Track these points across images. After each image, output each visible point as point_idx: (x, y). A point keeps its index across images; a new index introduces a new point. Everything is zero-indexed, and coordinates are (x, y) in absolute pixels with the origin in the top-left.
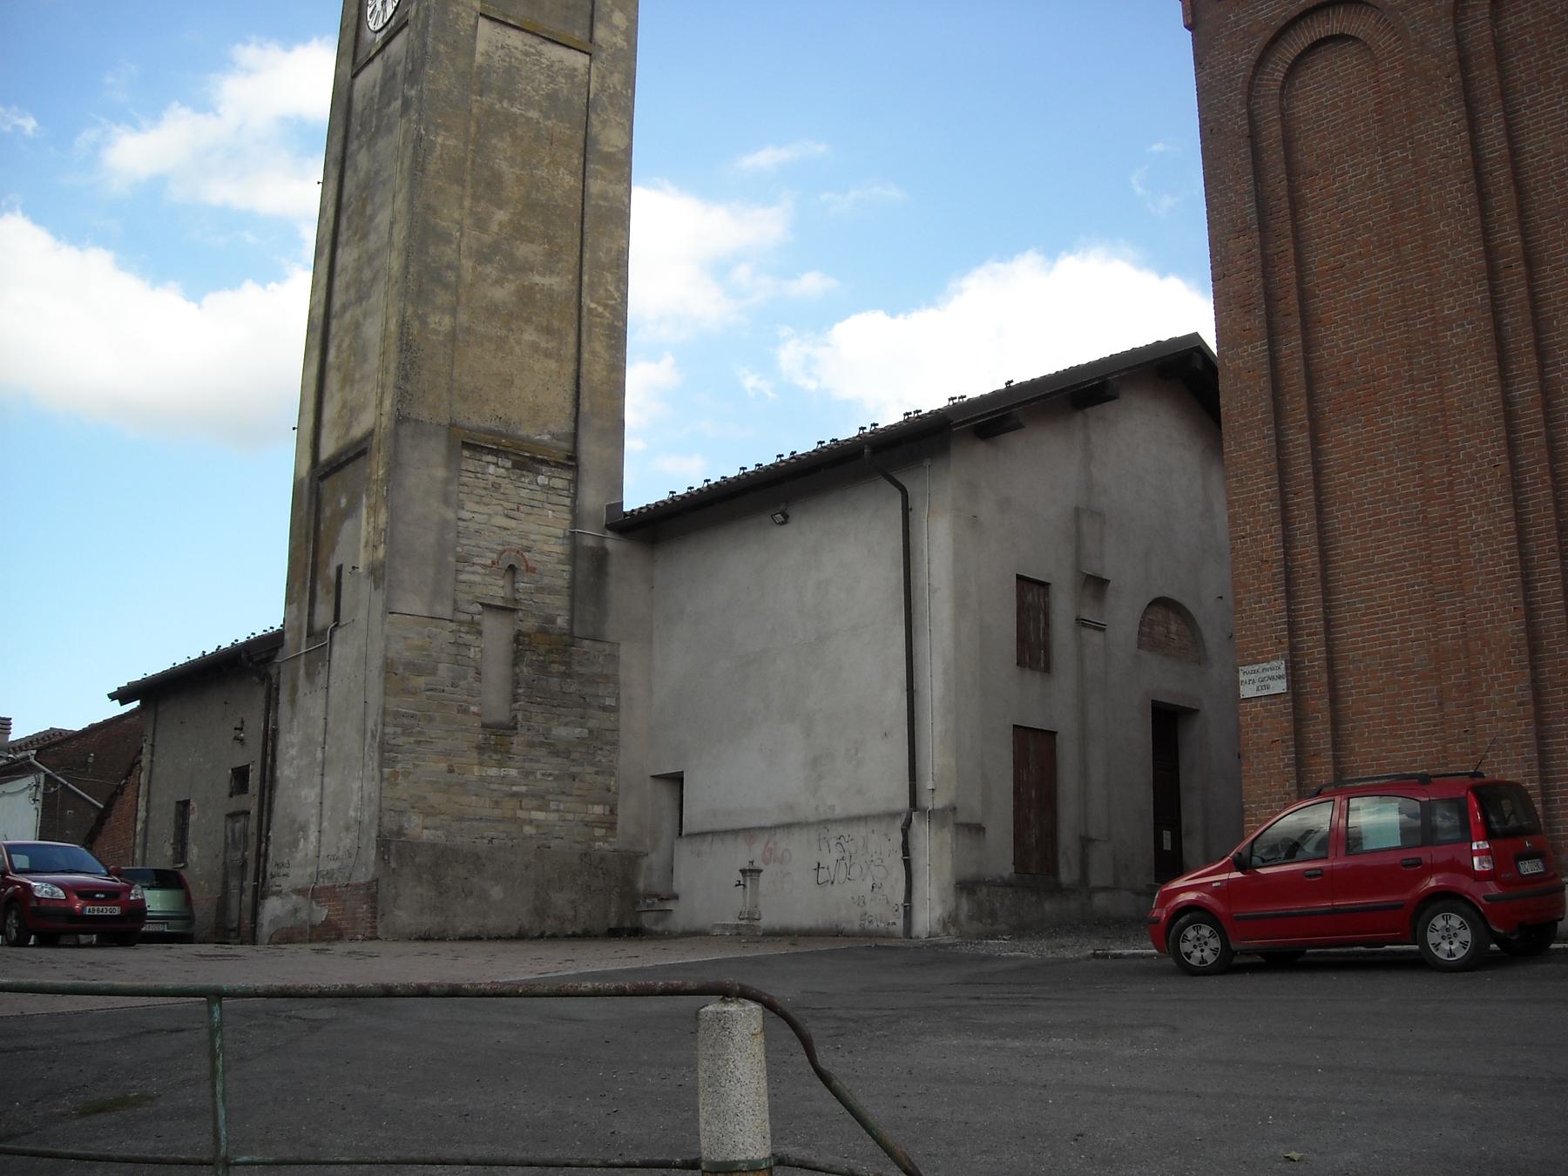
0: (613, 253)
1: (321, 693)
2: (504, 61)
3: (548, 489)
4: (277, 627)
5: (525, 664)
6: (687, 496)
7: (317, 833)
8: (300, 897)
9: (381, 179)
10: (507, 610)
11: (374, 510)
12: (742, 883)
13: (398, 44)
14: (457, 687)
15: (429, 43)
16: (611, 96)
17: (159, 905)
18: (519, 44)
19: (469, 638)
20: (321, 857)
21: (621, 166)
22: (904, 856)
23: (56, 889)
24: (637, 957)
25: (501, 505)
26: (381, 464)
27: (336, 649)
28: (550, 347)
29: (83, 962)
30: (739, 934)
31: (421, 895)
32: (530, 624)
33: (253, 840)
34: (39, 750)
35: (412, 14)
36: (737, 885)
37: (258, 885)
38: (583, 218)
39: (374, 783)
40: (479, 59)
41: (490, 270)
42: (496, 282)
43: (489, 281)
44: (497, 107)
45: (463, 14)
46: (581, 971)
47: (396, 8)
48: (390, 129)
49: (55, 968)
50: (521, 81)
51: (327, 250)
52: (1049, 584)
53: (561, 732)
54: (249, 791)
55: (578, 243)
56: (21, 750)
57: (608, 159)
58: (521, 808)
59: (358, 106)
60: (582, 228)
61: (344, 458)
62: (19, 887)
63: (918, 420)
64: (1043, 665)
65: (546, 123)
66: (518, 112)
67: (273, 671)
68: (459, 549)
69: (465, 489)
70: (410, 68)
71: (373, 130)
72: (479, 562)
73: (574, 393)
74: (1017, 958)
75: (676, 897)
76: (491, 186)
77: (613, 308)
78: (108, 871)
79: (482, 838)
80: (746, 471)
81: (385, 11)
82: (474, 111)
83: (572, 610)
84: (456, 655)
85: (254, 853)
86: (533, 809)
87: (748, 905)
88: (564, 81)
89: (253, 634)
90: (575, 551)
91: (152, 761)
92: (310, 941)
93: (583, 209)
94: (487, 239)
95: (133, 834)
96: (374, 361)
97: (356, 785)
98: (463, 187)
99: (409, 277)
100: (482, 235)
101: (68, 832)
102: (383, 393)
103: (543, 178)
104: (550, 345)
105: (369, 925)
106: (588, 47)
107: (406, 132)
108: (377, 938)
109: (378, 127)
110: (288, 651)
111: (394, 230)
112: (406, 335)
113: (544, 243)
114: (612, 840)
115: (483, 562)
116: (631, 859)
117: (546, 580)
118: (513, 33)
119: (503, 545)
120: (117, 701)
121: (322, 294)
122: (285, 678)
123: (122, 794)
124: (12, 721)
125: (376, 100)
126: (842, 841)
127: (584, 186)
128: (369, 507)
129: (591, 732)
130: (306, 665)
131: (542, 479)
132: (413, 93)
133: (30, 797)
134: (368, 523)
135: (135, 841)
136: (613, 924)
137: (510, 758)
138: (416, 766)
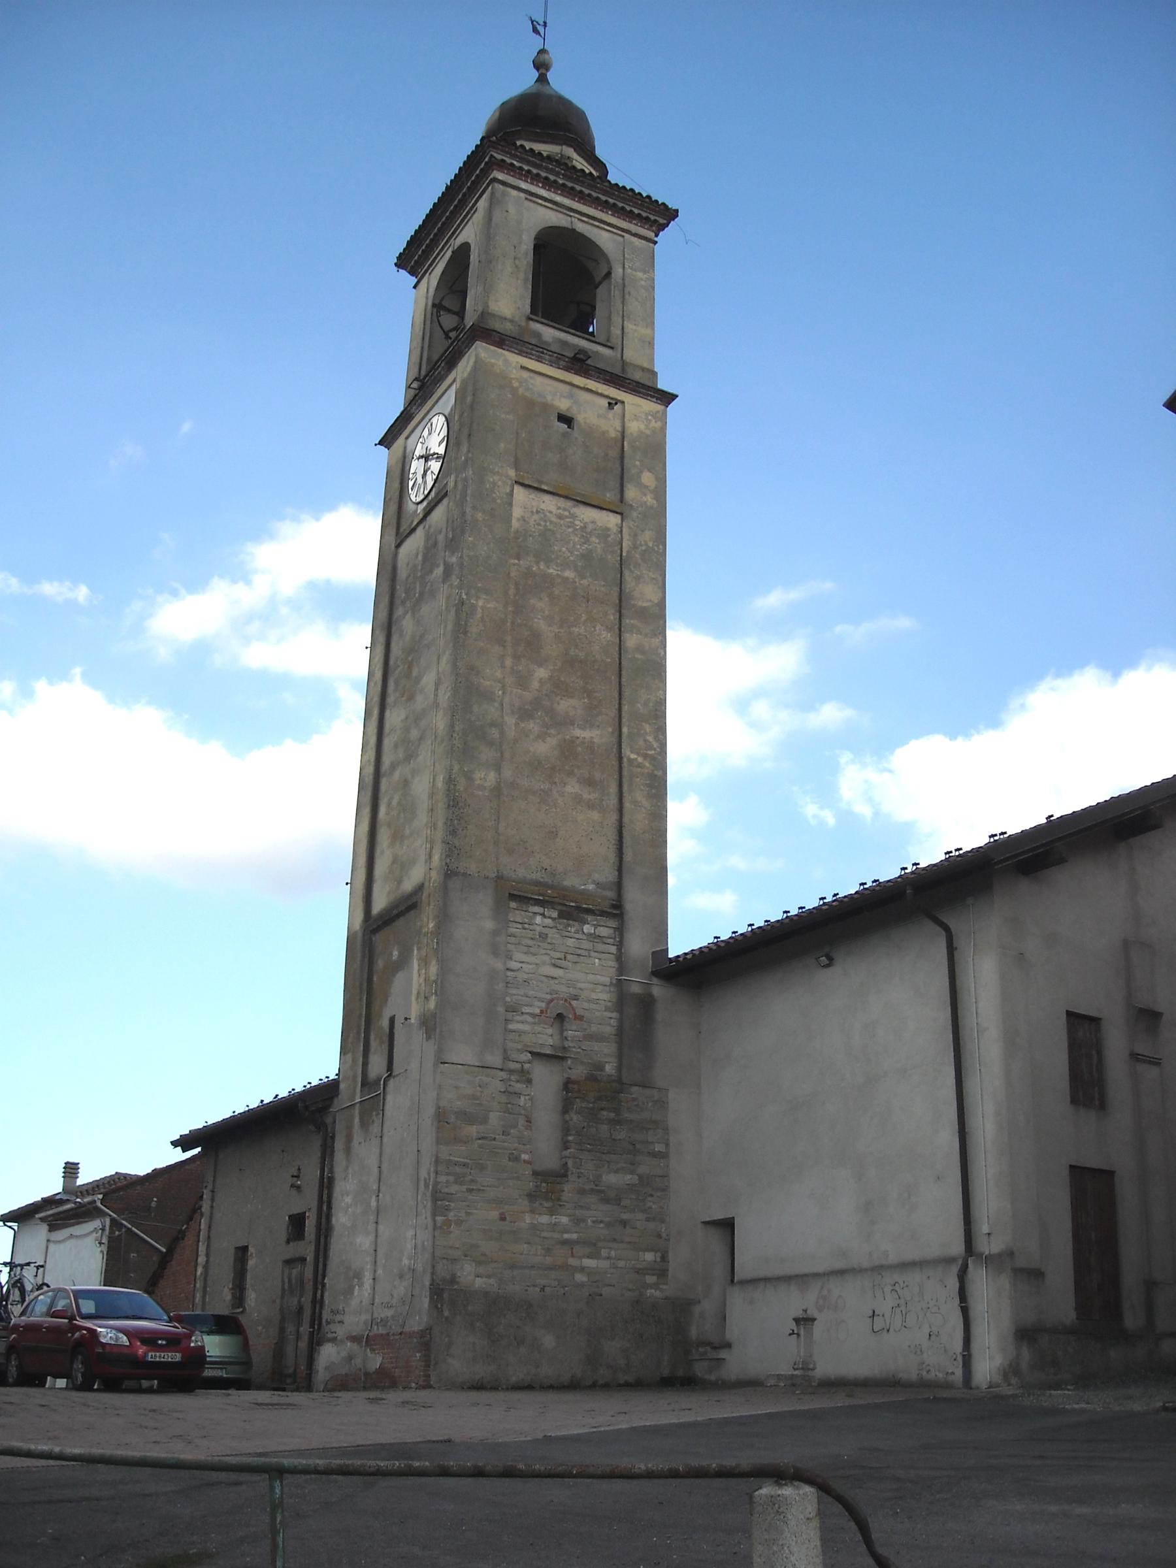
0: (651, 704)
1: (375, 1142)
2: (539, 525)
3: (594, 938)
4: (332, 1076)
5: (574, 1111)
6: (731, 941)
7: (371, 1281)
8: (355, 1344)
9: (426, 642)
10: (556, 1058)
11: (425, 962)
12: (795, 1332)
13: (438, 514)
14: (509, 1135)
15: (467, 512)
16: (643, 553)
17: (217, 1350)
18: (553, 508)
19: (519, 1087)
20: (376, 1305)
21: (656, 619)
22: (961, 1303)
23: (121, 1335)
24: (690, 1409)
25: (549, 955)
26: (431, 917)
27: (389, 1098)
28: (592, 798)
29: (145, 1409)
30: (794, 1385)
31: (474, 1343)
32: (578, 1072)
33: (309, 1286)
34: (105, 1195)
35: (451, 484)
36: (790, 1334)
37: (313, 1331)
38: (620, 671)
39: (427, 1231)
40: (515, 524)
41: (532, 725)
42: (538, 737)
43: (532, 737)
44: (534, 569)
45: (500, 483)
46: (634, 1425)
47: (436, 481)
48: (433, 594)
49: (118, 1414)
50: (556, 543)
51: (376, 712)
52: (1100, 1019)
53: (611, 1179)
54: (306, 1238)
55: (617, 696)
56: (88, 1194)
57: (642, 613)
58: (572, 1255)
59: (402, 573)
60: (620, 683)
61: (395, 912)
62: (85, 1332)
63: (959, 859)
64: (1097, 1103)
65: (582, 582)
66: (555, 573)
67: (329, 1120)
68: (508, 999)
69: (512, 940)
70: (451, 536)
71: (417, 595)
72: (528, 1011)
73: (617, 843)
74: (1082, 1411)
75: (728, 1346)
76: (531, 645)
77: (653, 759)
78: (169, 1317)
79: (534, 1286)
80: (789, 914)
81: (425, 483)
82: (513, 574)
83: (620, 1056)
84: (507, 1103)
85: (310, 1300)
86: (584, 1257)
87: (802, 1354)
88: (597, 541)
89: (310, 1083)
90: (622, 998)
91: (212, 1207)
92: (365, 1389)
93: (620, 664)
94: (528, 696)
95: (193, 1278)
96: (422, 818)
97: (410, 1233)
98: (504, 647)
99: (455, 735)
100: (524, 693)
101: (132, 1275)
102: (432, 848)
103: (580, 634)
104: (592, 796)
105: (422, 1373)
106: (619, 508)
107: (449, 597)
108: (430, 1387)
109: (422, 594)
110: (342, 1101)
111: (439, 691)
112: (453, 791)
113: (584, 698)
114: (664, 1287)
115: (531, 1011)
116: (682, 1307)
117: (594, 1028)
118: (547, 498)
119: (551, 994)
120: (179, 1148)
121: (372, 754)
122: (340, 1127)
123: (183, 1239)
124: (80, 1166)
125: (420, 568)
126: (897, 1287)
127: (620, 640)
128: (419, 959)
129: (640, 1177)
130: (360, 1115)
131: (587, 928)
132: (454, 559)
133: (96, 1240)
134: (419, 975)
135: (195, 1286)
136: (666, 1372)
137: (560, 1205)
138: (468, 1214)
